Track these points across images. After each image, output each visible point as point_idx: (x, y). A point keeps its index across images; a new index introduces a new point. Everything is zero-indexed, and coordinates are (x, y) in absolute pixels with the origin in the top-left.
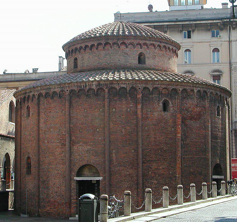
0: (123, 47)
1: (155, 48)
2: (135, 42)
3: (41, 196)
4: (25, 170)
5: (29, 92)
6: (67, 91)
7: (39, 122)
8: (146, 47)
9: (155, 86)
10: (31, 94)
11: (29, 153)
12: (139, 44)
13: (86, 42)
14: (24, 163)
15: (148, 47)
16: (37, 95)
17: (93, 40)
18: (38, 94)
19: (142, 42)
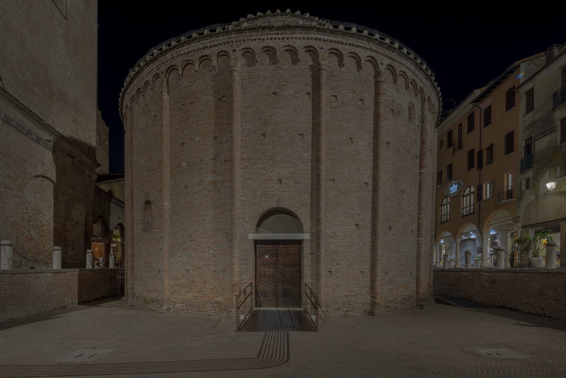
16: (163, 72)
18: (167, 71)
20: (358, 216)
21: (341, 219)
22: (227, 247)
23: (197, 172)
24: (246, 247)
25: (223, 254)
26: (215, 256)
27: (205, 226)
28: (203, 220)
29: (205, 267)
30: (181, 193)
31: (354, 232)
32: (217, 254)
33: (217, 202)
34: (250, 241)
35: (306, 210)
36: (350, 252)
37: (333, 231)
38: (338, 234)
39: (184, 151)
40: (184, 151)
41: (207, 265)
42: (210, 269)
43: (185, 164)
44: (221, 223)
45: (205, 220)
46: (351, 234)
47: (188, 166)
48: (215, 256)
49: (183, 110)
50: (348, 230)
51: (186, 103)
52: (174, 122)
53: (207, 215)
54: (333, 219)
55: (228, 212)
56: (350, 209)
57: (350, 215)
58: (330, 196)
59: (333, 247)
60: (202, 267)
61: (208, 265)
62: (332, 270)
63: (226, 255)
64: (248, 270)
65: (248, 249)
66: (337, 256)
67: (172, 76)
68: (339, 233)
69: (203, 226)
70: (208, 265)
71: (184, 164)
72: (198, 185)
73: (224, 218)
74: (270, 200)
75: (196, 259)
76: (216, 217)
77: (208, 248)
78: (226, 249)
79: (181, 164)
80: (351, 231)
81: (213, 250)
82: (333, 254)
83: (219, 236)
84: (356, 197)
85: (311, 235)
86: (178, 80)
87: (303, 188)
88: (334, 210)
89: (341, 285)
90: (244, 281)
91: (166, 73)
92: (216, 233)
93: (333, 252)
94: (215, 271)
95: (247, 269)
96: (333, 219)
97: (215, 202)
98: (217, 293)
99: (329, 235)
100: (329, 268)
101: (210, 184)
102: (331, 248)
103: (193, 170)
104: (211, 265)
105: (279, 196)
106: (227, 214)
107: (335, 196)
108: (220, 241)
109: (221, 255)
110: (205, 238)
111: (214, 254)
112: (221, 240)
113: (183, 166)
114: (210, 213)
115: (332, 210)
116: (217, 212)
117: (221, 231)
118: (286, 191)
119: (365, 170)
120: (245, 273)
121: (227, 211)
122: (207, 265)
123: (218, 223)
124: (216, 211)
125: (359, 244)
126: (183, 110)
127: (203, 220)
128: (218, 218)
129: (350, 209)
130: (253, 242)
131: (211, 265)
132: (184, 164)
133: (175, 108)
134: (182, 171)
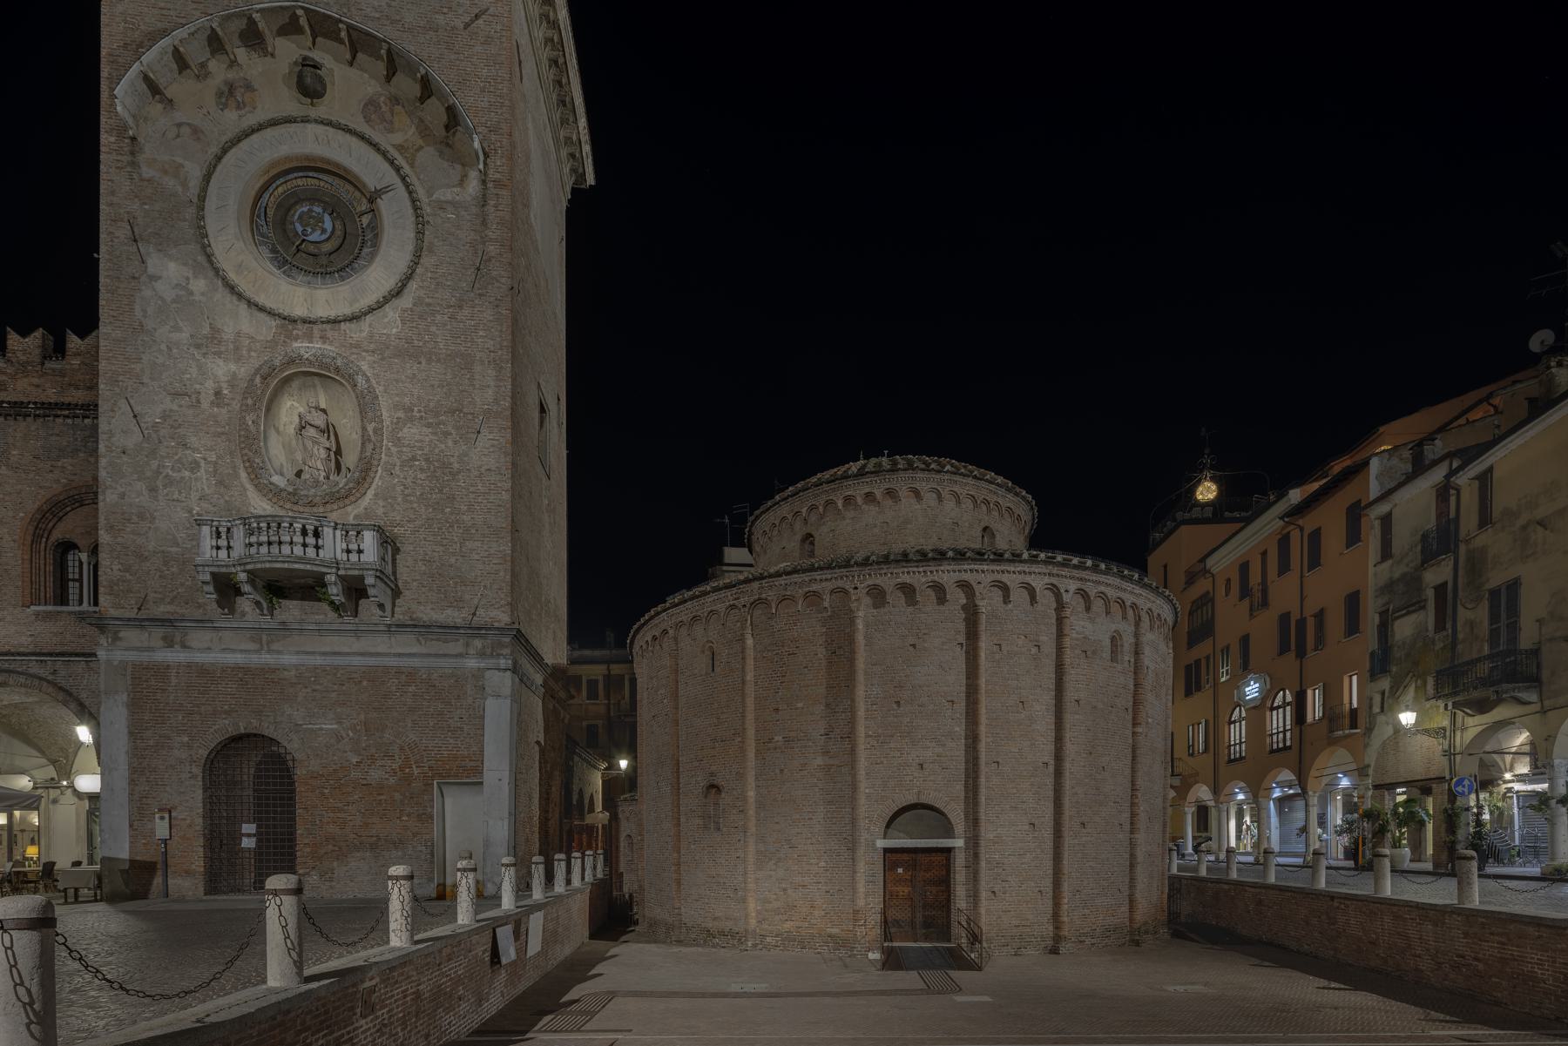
36: (1022, 864)
39: (778, 720)
40: (778, 720)
45: (811, 819)
53: (815, 812)
62: (995, 889)
71: (778, 738)
76: (829, 816)
85: (965, 841)
89: (1009, 911)
100: (992, 887)
113: (778, 741)
118: (930, 780)
121: (845, 808)
132: (778, 738)
134: (775, 749)
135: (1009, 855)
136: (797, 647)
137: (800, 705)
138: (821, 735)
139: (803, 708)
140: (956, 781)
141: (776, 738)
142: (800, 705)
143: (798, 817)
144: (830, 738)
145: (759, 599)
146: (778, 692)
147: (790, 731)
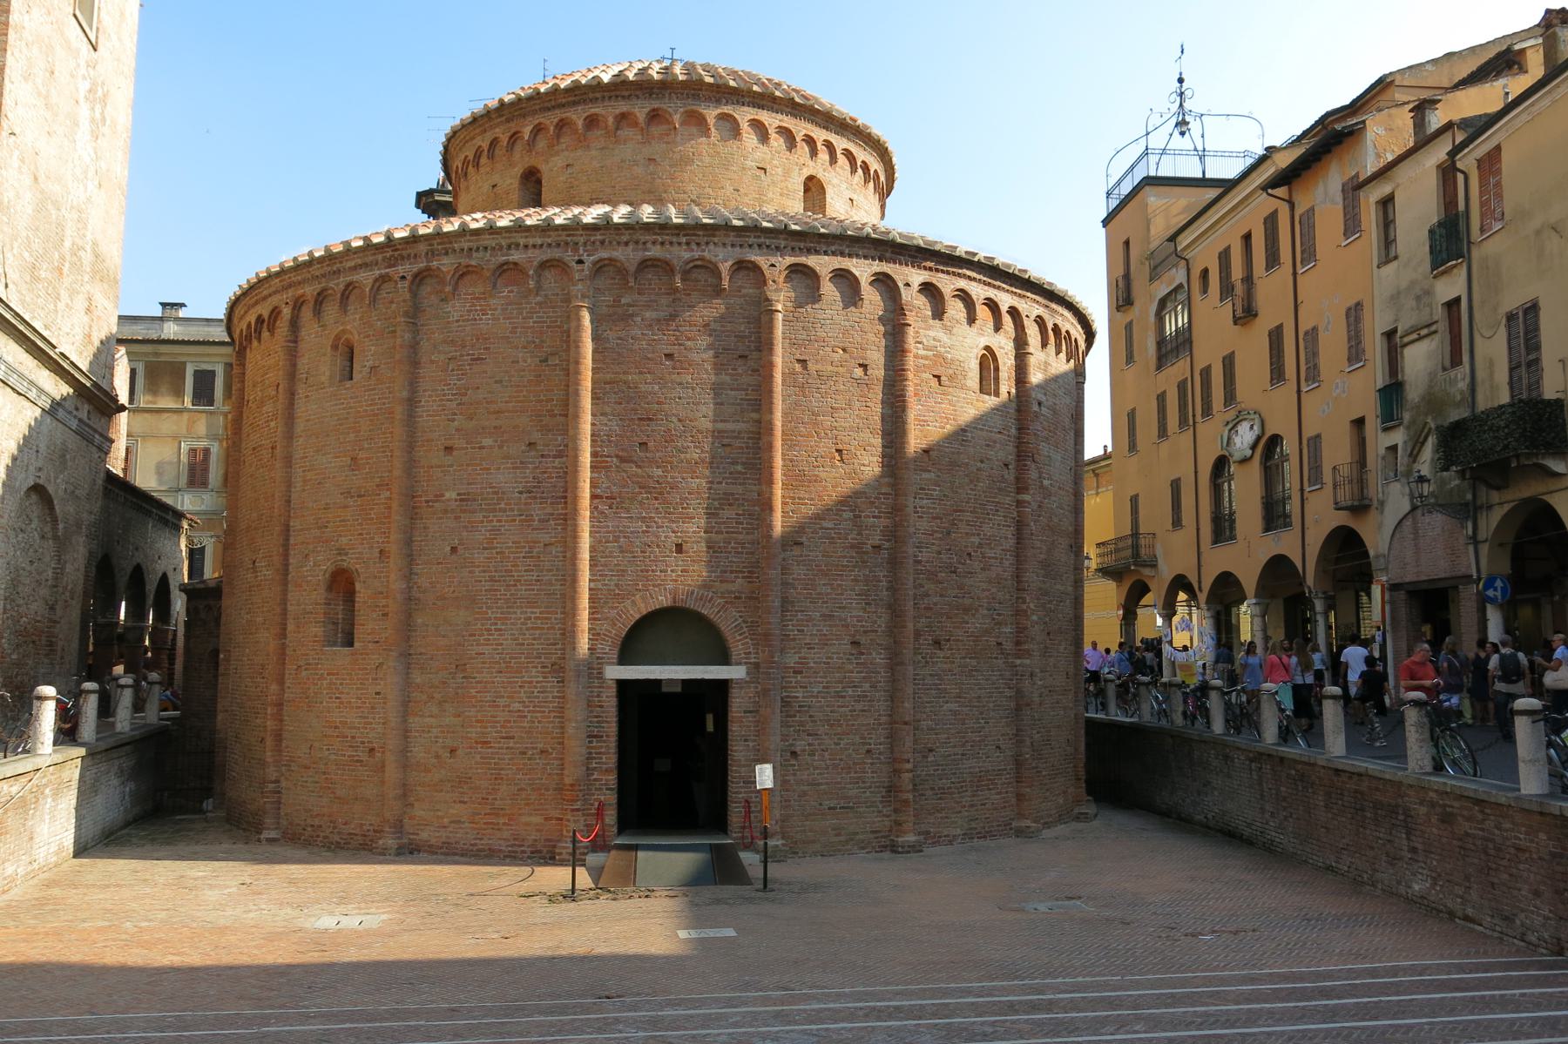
0: (750, 138)
1: (854, 171)
2: (801, 128)
3: (418, 753)
4: (309, 631)
5: (355, 268)
6: (580, 262)
7: (412, 402)
8: (827, 157)
9: (962, 284)
10: (366, 278)
11: (341, 551)
12: (810, 141)
13: (594, 100)
14: (309, 596)
15: (833, 160)
16: (403, 278)
17: (627, 94)
18: (416, 276)
19: (820, 135)
20: (858, 621)
21: (818, 630)
22: (553, 697)
23: (484, 517)
24: (598, 696)
25: (544, 712)
26: (525, 717)
27: (502, 644)
28: (496, 630)
29: (500, 742)
30: (442, 563)
31: (848, 659)
32: (529, 712)
33: (533, 590)
34: (610, 682)
35: (739, 612)
36: (839, 706)
37: (800, 658)
38: (812, 665)
39: (452, 466)
40: (452, 466)
41: (503, 738)
42: (512, 748)
43: (454, 495)
44: (540, 639)
45: (500, 630)
46: (843, 663)
47: (461, 500)
48: (525, 717)
49: (453, 370)
50: (835, 656)
51: (462, 355)
52: (427, 394)
53: (506, 618)
54: (798, 630)
55: (559, 616)
56: (840, 608)
57: (840, 620)
58: (793, 579)
59: (800, 695)
60: (490, 743)
61: (507, 738)
62: (798, 749)
63: (553, 714)
64: (603, 750)
65: (604, 701)
66: (811, 716)
67: (426, 289)
68: (814, 663)
69: (497, 645)
70: (507, 738)
72: (485, 549)
73: (548, 629)
74: (656, 589)
75: (477, 721)
76: (529, 625)
77: (508, 697)
78: (551, 702)
79: (443, 495)
80: (841, 658)
81: (519, 702)
82: (799, 712)
83: (534, 670)
84: (852, 580)
85: (748, 668)
86: (442, 300)
87: (731, 562)
88: (803, 611)
89: (819, 784)
90: (595, 777)
91: (412, 282)
92: (528, 663)
93: (800, 706)
94: (525, 753)
95: (602, 747)
96: (798, 630)
97: (526, 590)
98: (527, 804)
99: (791, 668)
100: (792, 745)
101: (517, 547)
102: (797, 697)
103: (474, 512)
104: (513, 738)
105: (676, 581)
106: (556, 619)
107: (804, 579)
108: (537, 682)
109: (539, 715)
110: (501, 672)
111: (523, 712)
112: (541, 679)
114: (513, 616)
115: (796, 611)
116: (532, 613)
117: (540, 658)
119: (874, 517)
120: (595, 758)
122: (503, 738)
123: (534, 639)
124: (529, 610)
125: (861, 687)
126: (453, 370)
127: (496, 630)
128: (532, 628)
129: (840, 608)
130: (615, 685)
131: (513, 738)
132: (451, 495)
133: (432, 362)
134: (446, 511)
135: (819, 692)
136: (486, 349)
137: (487, 442)
138: (521, 493)
139: (491, 447)
140: (732, 572)
141: (447, 495)
142: (487, 442)
143: (479, 626)
144: (535, 498)
145: (428, 269)
146: (453, 420)
147: (468, 484)
